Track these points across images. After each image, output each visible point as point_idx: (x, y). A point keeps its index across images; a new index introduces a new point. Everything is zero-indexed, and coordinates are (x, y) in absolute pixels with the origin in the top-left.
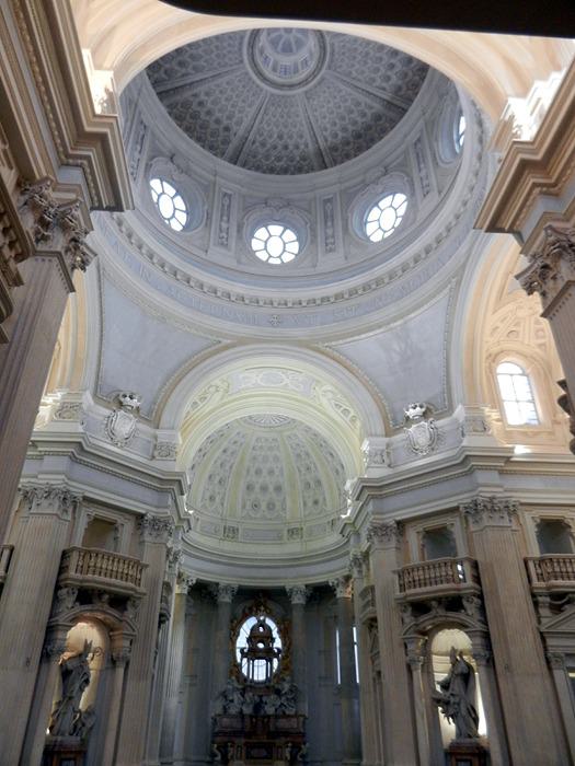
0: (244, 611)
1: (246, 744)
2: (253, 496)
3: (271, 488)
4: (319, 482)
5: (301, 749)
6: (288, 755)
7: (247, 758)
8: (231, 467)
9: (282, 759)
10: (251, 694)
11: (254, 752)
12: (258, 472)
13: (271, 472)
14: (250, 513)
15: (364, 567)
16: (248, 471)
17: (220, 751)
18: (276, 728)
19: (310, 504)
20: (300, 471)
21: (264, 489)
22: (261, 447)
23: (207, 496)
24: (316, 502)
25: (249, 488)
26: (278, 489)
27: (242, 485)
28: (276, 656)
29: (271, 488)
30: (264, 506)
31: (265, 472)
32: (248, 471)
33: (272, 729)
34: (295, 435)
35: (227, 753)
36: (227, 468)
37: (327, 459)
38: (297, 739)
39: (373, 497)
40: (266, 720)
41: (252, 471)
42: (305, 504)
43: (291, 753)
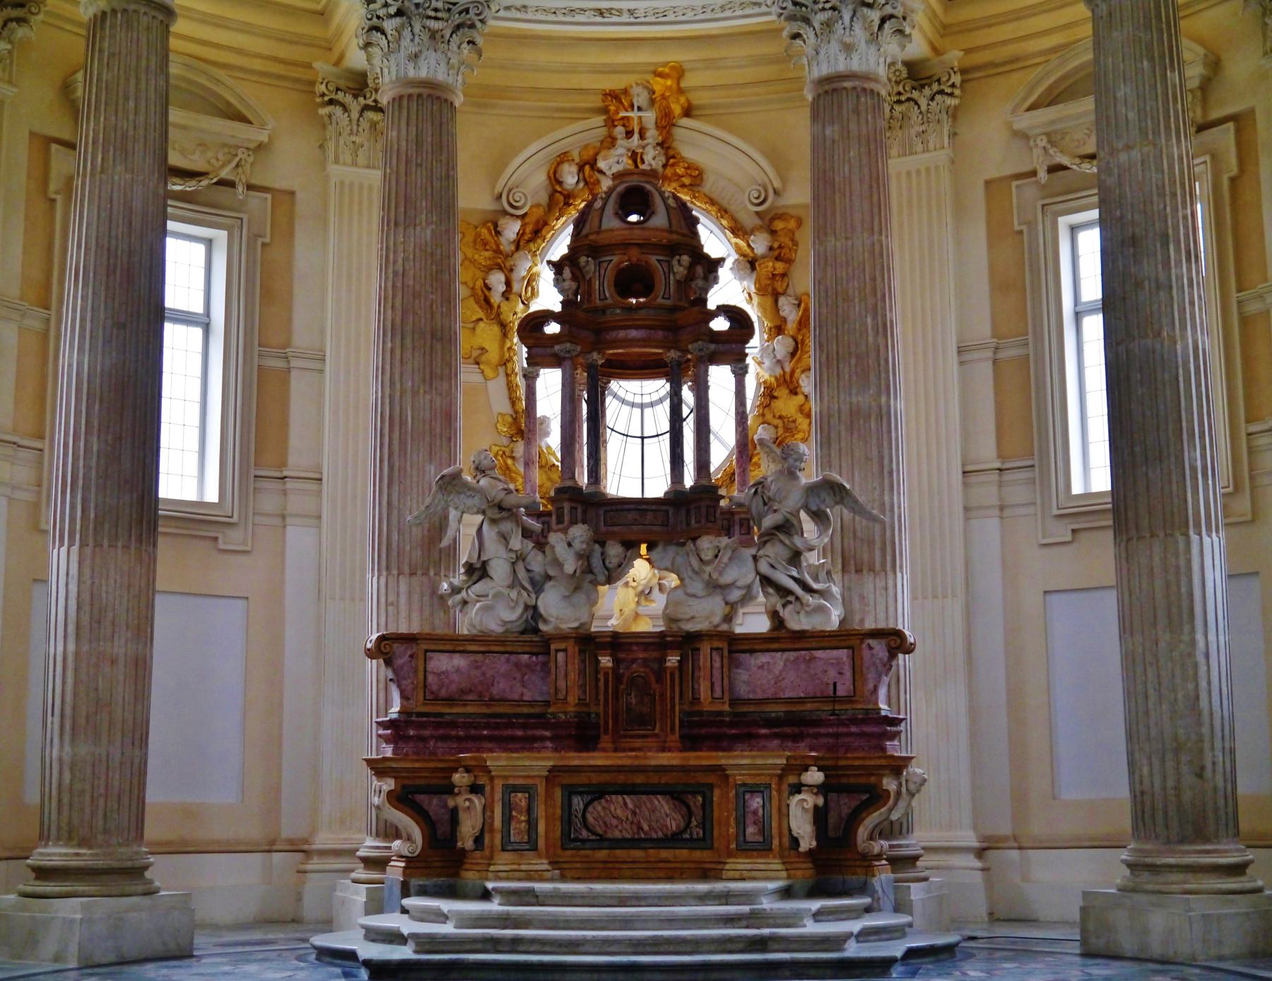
0: (555, 179)
1: (552, 770)
5: (876, 797)
6: (802, 826)
7: (568, 839)
9: (763, 848)
10: (579, 532)
11: (615, 813)
17: (420, 814)
18: (734, 702)
28: (730, 348)
33: (707, 695)
35: (454, 816)
38: (850, 750)
40: (673, 660)
43: (820, 816)
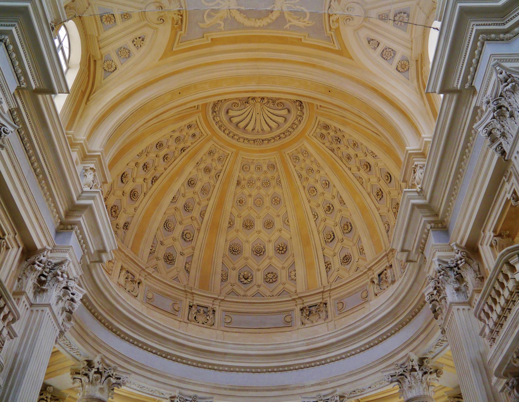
2: (240, 263)
3: (270, 250)
4: (348, 227)
8: (202, 215)
12: (248, 225)
13: (269, 225)
14: (234, 287)
15: (469, 276)
16: (231, 224)
19: (336, 262)
20: (316, 216)
21: (259, 252)
22: (251, 183)
23: (161, 252)
24: (346, 260)
25: (235, 250)
26: (282, 250)
27: (222, 245)
29: (270, 250)
30: (259, 277)
31: (259, 225)
32: (231, 224)
34: (306, 153)
36: (196, 213)
37: (359, 179)
39: (490, 37)
41: (238, 223)
42: (328, 266)
